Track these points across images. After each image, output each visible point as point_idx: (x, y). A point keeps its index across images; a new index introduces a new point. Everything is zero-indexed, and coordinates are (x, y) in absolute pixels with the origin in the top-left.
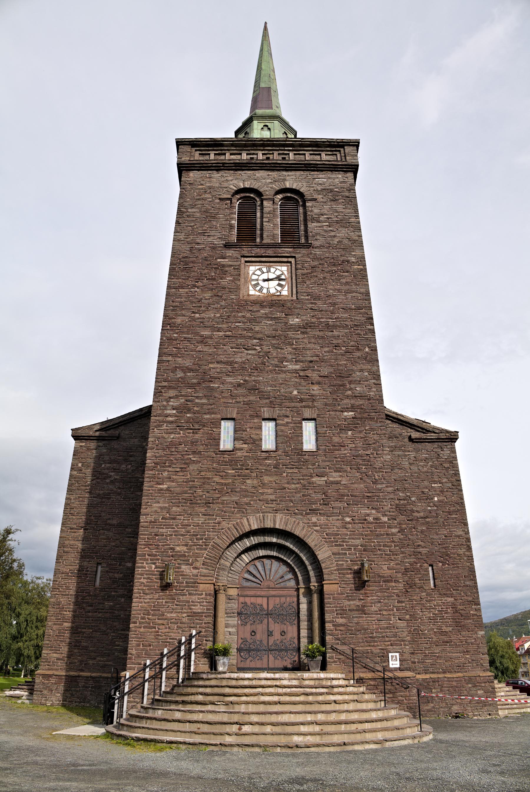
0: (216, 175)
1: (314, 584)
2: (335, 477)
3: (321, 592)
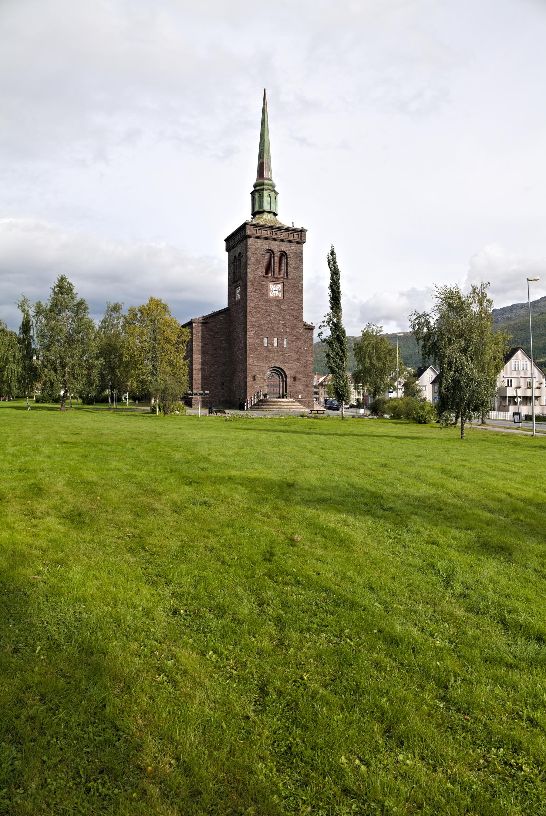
0: (259, 241)
1: (284, 379)
2: (291, 354)
3: (286, 381)
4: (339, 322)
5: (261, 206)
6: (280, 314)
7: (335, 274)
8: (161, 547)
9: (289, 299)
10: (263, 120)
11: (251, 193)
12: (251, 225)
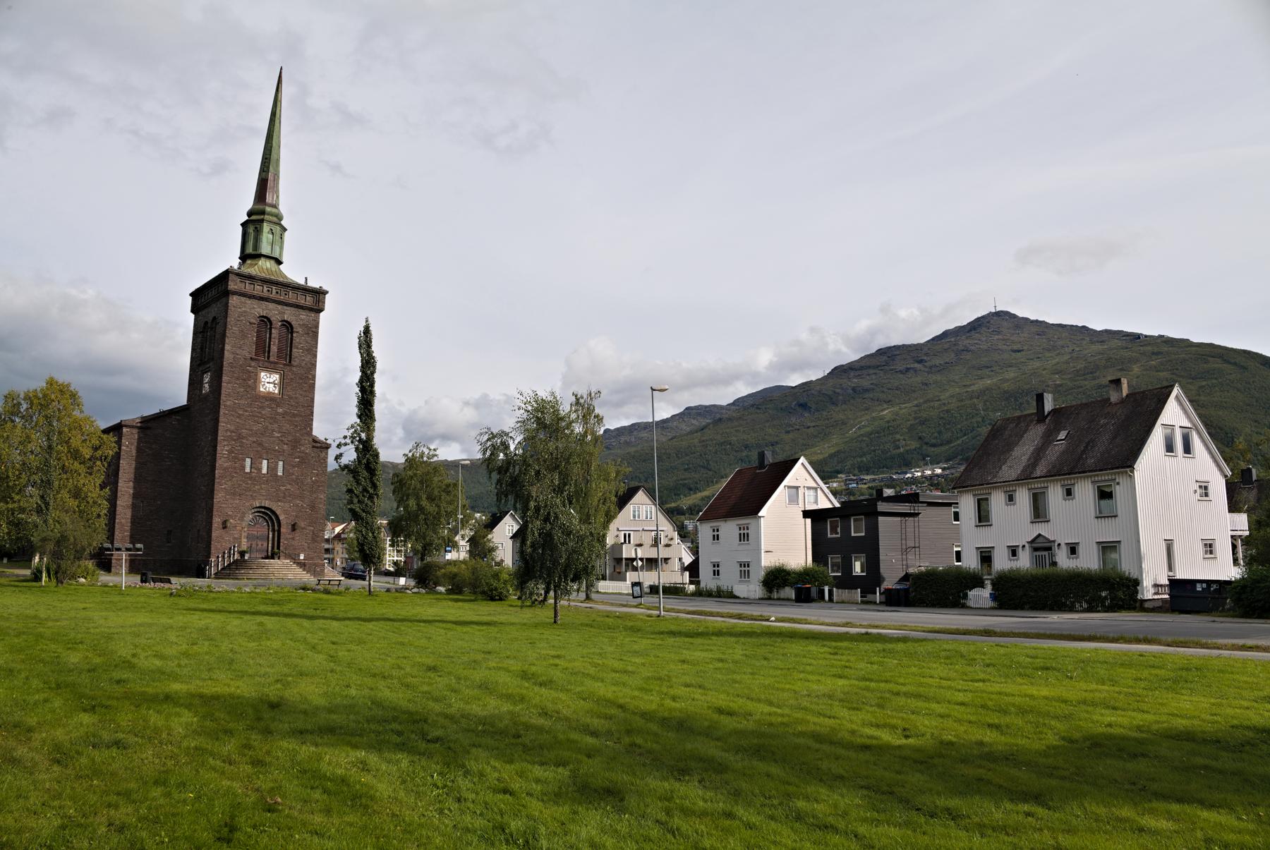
0: (249, 301)
4: (370, 439)
5: (256, 246)
6: (275, 421)
7: (368, 365)
8: (19, 832)
9: (291, 398)
10: (273, 114)
11: (242, 225)
12: (238, 275)
